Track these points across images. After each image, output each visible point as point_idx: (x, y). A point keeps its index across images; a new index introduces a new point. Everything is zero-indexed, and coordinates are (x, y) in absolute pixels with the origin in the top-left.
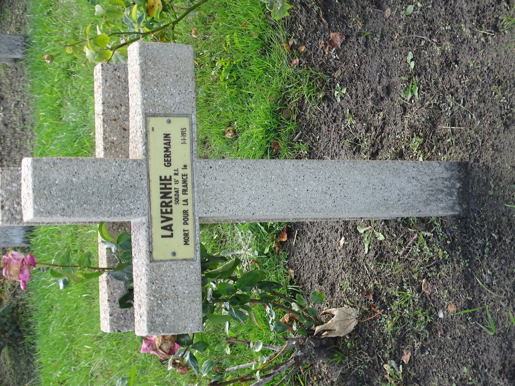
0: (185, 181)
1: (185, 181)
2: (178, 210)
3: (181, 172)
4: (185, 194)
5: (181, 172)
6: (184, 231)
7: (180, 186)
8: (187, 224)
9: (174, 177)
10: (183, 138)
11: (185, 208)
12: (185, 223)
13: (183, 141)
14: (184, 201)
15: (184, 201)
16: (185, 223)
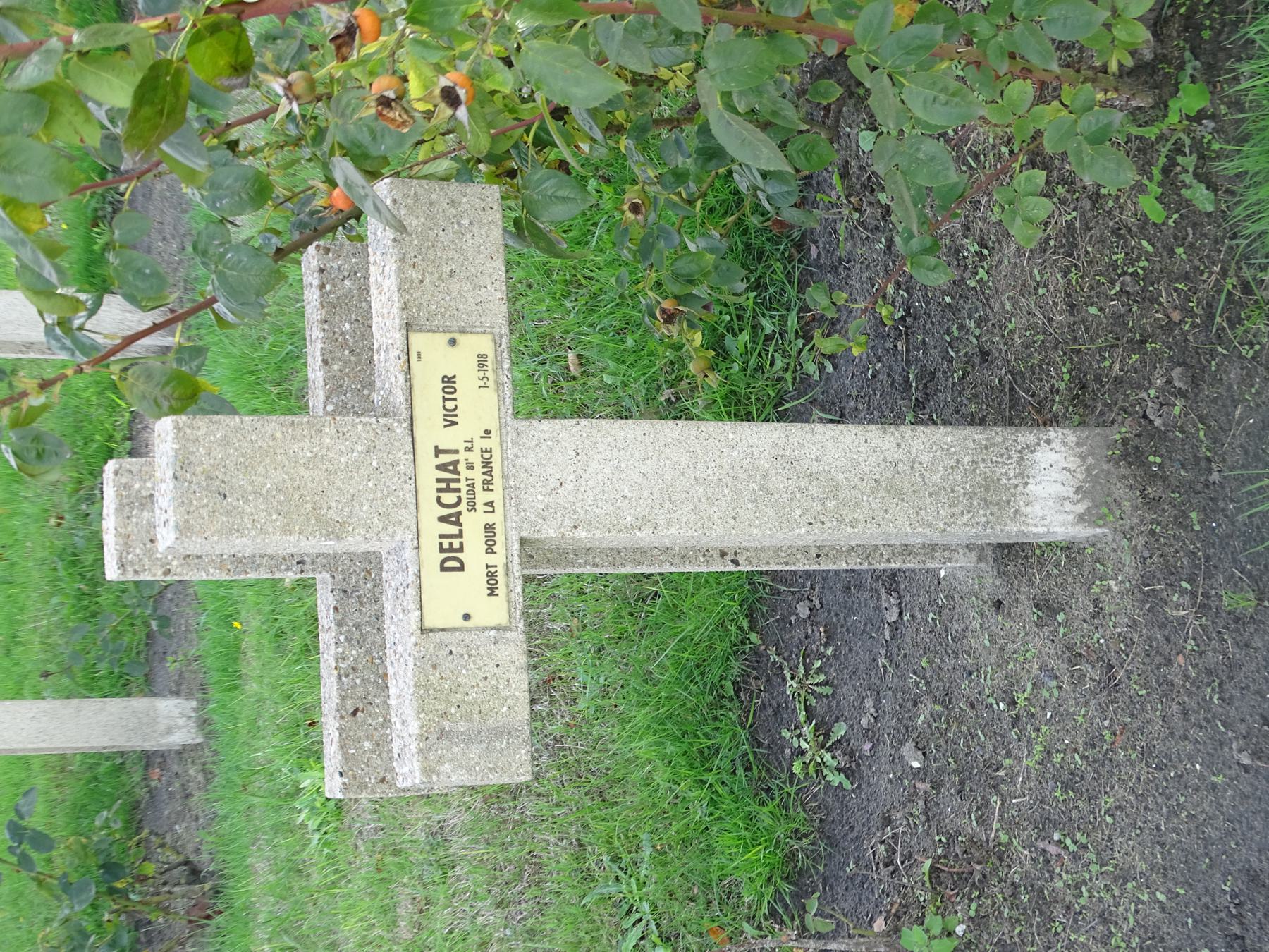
0: (487, 464)
1: (487, 464)
2: (473, 524)
3: (479, 444)
4: (488, 490)
5: (479, 444)
6: (488, 566)
7: (478, 475)
8: (493, 552)
9: (462, 456)
10: (481, 374)
11: (490, 519)
12: (490, 550)
13: (482, 383)
14: (486, 504)
15: (486, 504)
16: (490, 550)
